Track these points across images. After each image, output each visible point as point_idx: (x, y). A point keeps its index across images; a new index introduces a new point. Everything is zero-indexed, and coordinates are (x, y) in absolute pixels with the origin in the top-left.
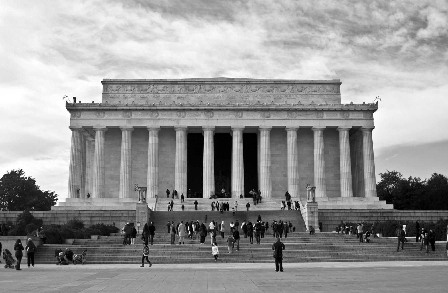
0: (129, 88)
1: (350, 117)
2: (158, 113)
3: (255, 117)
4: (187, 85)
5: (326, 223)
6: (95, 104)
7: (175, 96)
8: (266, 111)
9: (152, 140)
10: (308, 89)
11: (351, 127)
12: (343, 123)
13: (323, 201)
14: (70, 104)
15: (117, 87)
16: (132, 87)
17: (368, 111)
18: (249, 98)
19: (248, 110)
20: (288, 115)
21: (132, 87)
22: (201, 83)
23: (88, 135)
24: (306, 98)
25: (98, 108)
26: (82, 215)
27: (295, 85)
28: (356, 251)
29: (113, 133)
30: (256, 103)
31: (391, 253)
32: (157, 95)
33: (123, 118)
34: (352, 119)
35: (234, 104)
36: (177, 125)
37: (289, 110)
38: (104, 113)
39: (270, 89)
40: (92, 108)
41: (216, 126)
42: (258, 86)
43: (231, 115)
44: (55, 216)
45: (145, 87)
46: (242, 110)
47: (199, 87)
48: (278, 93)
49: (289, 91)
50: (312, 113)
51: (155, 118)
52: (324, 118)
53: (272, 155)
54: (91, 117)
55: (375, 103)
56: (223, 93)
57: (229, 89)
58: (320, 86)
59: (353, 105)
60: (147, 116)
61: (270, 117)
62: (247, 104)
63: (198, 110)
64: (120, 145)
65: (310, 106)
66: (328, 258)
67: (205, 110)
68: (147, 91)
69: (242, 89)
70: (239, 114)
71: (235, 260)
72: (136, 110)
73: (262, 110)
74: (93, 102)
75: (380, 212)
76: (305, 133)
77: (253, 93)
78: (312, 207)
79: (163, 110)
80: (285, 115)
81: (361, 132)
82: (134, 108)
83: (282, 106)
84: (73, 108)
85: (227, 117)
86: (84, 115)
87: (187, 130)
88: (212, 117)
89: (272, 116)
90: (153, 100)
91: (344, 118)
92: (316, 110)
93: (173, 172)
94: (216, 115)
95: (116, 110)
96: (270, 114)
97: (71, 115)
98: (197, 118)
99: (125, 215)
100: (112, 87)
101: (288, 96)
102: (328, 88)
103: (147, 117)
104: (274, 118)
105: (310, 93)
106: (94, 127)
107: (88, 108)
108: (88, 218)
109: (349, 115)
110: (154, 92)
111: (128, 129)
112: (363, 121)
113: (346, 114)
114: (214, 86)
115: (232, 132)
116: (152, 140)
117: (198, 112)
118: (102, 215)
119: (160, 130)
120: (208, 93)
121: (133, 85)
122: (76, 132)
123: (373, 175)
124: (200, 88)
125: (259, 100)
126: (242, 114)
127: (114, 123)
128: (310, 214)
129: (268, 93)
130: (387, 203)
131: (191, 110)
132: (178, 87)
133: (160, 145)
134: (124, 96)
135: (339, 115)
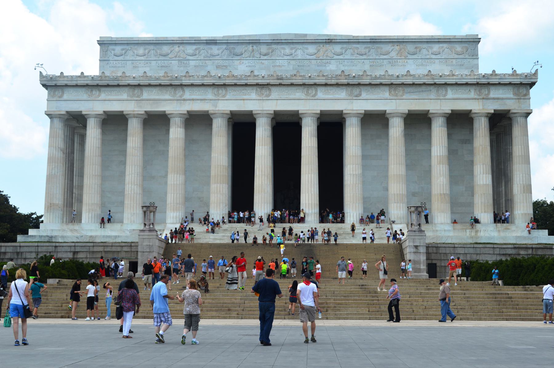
0: (141, 50)
1: (492, 95)
2: (184, 91)
3: (337, 96)
4: (232, 46)
5: (443, 264)
6: (85, 77)
7: (214, 63)
8: (354, 86)
9: (176, 132)
10: (425, 51)
11: (493, 112)
12: (479, 106)
13: (442, 229)
14: (46, 77)
15: (123, 50)
16: (145, 49)
17: (521, 84)
18: (331, 66)
19: (326, 85)
20: (390, 92)
21: (145, 49)
22: (254, 42)
23: (78, 125)
24: (422, 65)
25: (90, 83)
26: (59, 249)
27: (404, 44)
28: (412, 304)
29: (114, 122)
30: (339, 73)
31: (467, 307)
32: (185, 62)
33: (129, 98)
34: (494, 99)
36: (214, 109)
37: (392, 84)
38: (100, 91)
40: (80, 83)
41: (274, 111)
42: (345, 46)
43: (299, 93)
44: (18, 251)
45: (166, 49)
46: (315, 85)
47: (251, 48)
48: (377, 57)
49: (393, 54)
50: (429, 88)
52: (448, 97)
53: (364, 157)
54: (80, 98)
55: (533, 72)
56: (288, 57)
57: (299, 52)
58: (445, 45)
59: (496, 75)
60: (166, 95)
61: (360, 95)
62: (323, 76)
63: (246, 85)
64: (125, 141)
65: (426, 78)
66: (363, 314)
67: (257, 85)
68: (170, 56)
69: (319, 51)
70: (312, 91)
71: (214, 314)
72: (150, 85)
73: (348, 85)
74: (82, 73)
75: (532, 248)
76: (417, 121)
78: (416, 237)
79: (192, 85)
80: (385, 93)
81: (510, 119)
82: (146, 82)
83: (380, 77)
85: (292, 97)
86: (69, 94)
87: (229, 116)
88: (269, 95)
89: (364, 95)
90: (177, 71)
91: (481, 97)
92: (435, 84)
93: (207, 183)
94: (275, 93)
95: (118, 86)
96: (360, 92)
97: (49, 94)
98: (245, 97)
99: (125, 249)
100: (114, 50)
101: (392, 62)
102: (459, 48)
103: (167, 97)
105: (428, 57)
106: (84, 113)
107: (74, 83)
108: (69, 254)
109: (489, 94)
110: (179, 57)
111: (136, 116)
112: (513, 101)
113: (485, 91)
114: (274, 46)
115: (301, 119)
116: (176, 132)
117: (247, 88)
118: (91, 249)
119: (187, 116)
120: (265, 58)
121: (147, 47)
122: (56, 121)
123: (528, 189)
124: (253, 50)
125: (343, 68)
126: (316, 91)
127: (115, 107)
128: (413, 250)
129: (361, 57)
130: (549, 235)
131: (236, 85)
132: (218, 49)
133: (189, 141)
134: (133, 63)
135: (472, 93)
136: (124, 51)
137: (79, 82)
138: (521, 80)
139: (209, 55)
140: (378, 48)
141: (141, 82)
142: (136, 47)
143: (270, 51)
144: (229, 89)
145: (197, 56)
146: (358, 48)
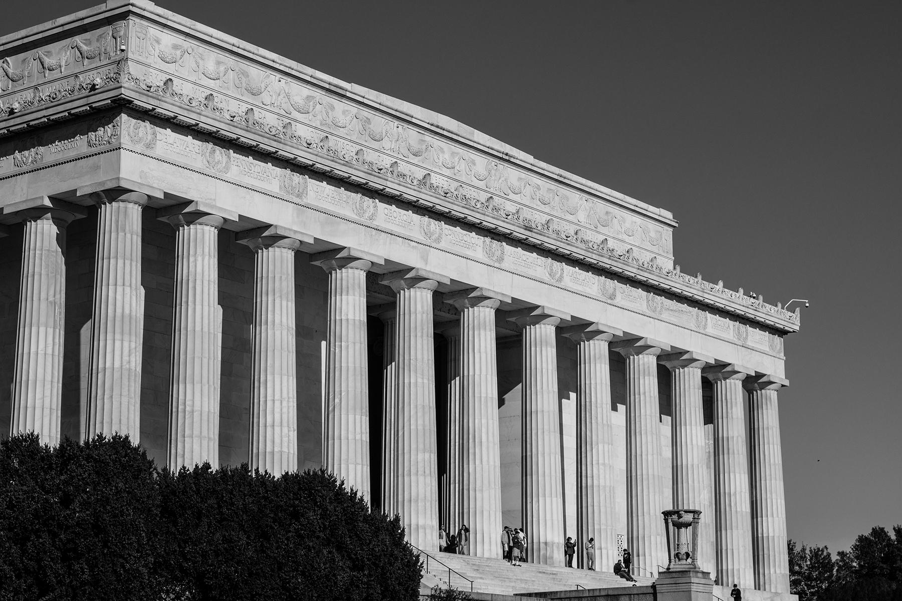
4: (366, 113)
16: (219, 63)
35: (558, 233)
39: (547, 197)
51: (368, 223)
56: (447, 172)
77: (512, 196)
85: (531, 273)
91: (740, 343)
98: (469, 253)
100: (158, 41)
105: (620, 237)
114: (429, 138)
120: (415, 160)
136: (178, 53)
137: (203, 119)
139: (329, 121)
141: (319, 160)
142: (201, 50)
143: (424, 147)
145: (310, 116)
146: (538, 188)
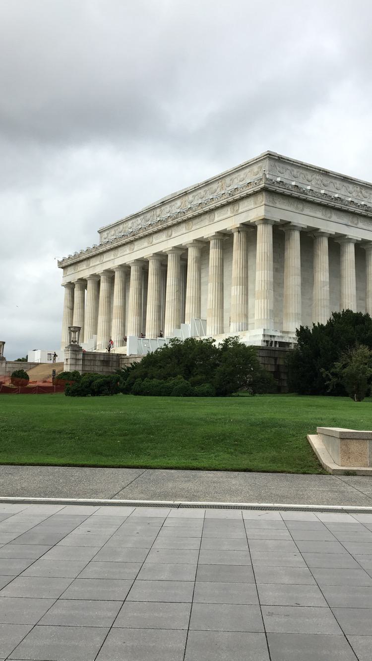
1: (240, 211)
9: (104, 286)
42: (194, 194)
58: (247, 170)
80: (183, 229)
84: (65, 266)
85: (143, 247)
86: (70, 270)
88: (133, 249)
89: (173, 235)
92: (206, 213)
98: (125, 253)
104: (176, 235)
109: (238, 209)
114: (163, 208)
135: (228, 211)
138: (254, 189)
140: (211, 188)
144: (119, 249)
